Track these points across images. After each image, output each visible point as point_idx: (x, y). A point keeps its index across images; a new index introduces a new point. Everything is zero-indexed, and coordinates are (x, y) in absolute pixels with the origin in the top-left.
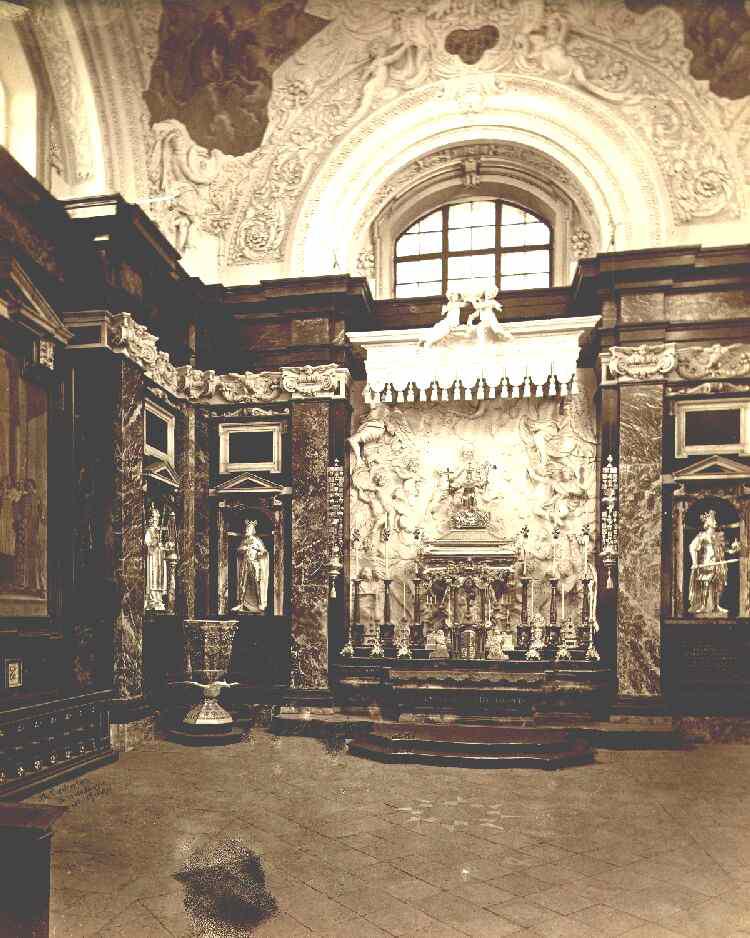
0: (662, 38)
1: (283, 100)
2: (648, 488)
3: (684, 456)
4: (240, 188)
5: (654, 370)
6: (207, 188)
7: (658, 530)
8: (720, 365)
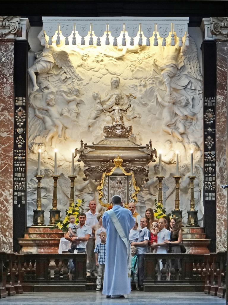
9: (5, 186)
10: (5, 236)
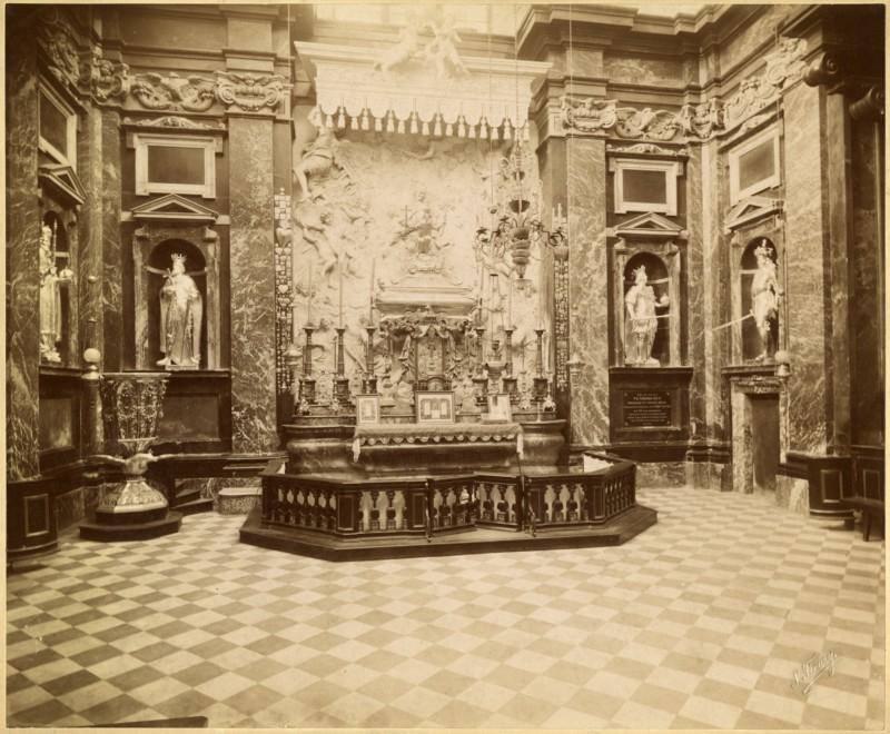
2: (595, 239)
3: (624, 212)
5: (598, 125)
7: (604, 281)
8: (650, 128)
9: (262, 344)
10: (264, 421)
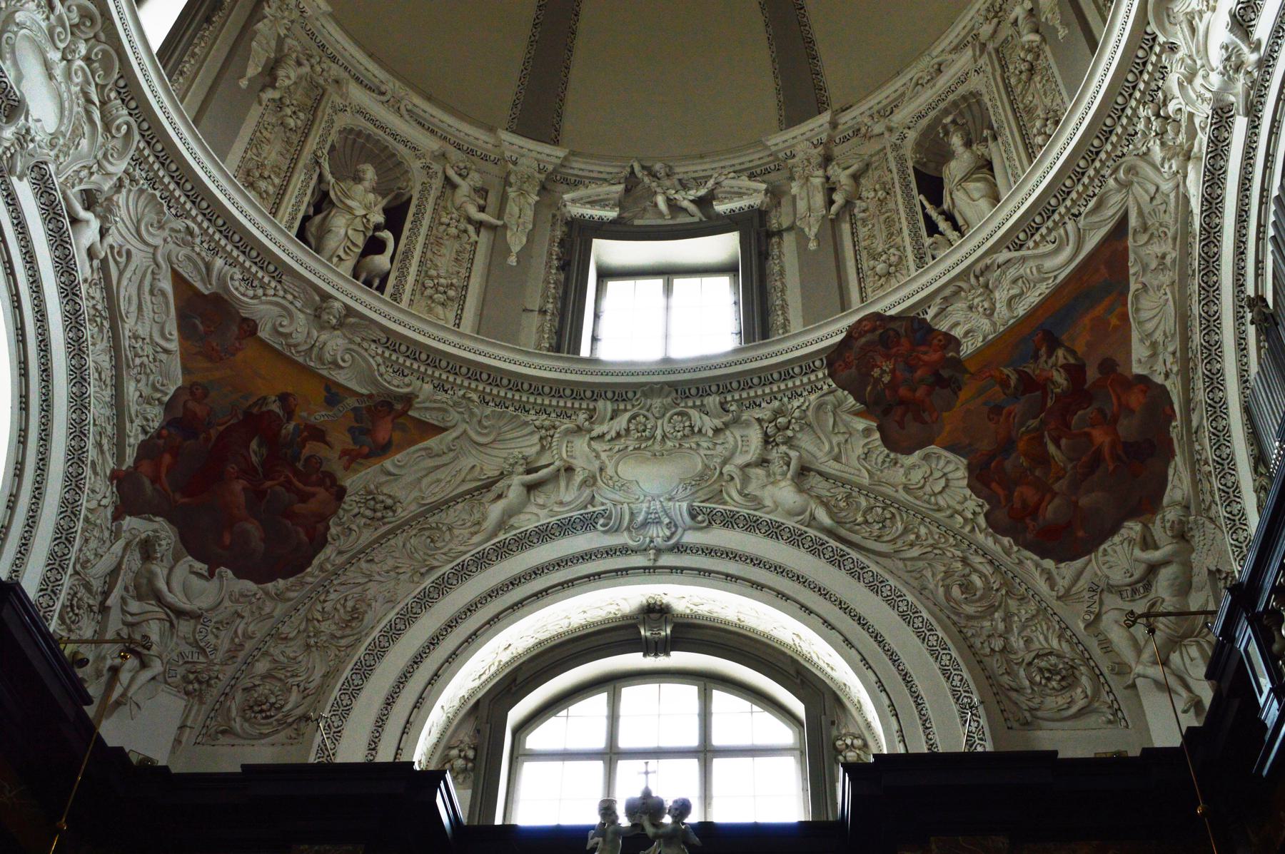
0: (942, 482)
1: (355, 516)
4: (251, 628)
6: (193, 622)
